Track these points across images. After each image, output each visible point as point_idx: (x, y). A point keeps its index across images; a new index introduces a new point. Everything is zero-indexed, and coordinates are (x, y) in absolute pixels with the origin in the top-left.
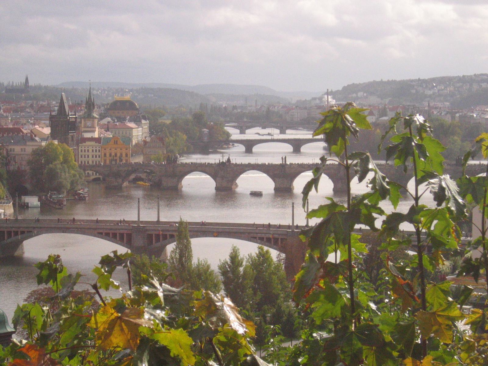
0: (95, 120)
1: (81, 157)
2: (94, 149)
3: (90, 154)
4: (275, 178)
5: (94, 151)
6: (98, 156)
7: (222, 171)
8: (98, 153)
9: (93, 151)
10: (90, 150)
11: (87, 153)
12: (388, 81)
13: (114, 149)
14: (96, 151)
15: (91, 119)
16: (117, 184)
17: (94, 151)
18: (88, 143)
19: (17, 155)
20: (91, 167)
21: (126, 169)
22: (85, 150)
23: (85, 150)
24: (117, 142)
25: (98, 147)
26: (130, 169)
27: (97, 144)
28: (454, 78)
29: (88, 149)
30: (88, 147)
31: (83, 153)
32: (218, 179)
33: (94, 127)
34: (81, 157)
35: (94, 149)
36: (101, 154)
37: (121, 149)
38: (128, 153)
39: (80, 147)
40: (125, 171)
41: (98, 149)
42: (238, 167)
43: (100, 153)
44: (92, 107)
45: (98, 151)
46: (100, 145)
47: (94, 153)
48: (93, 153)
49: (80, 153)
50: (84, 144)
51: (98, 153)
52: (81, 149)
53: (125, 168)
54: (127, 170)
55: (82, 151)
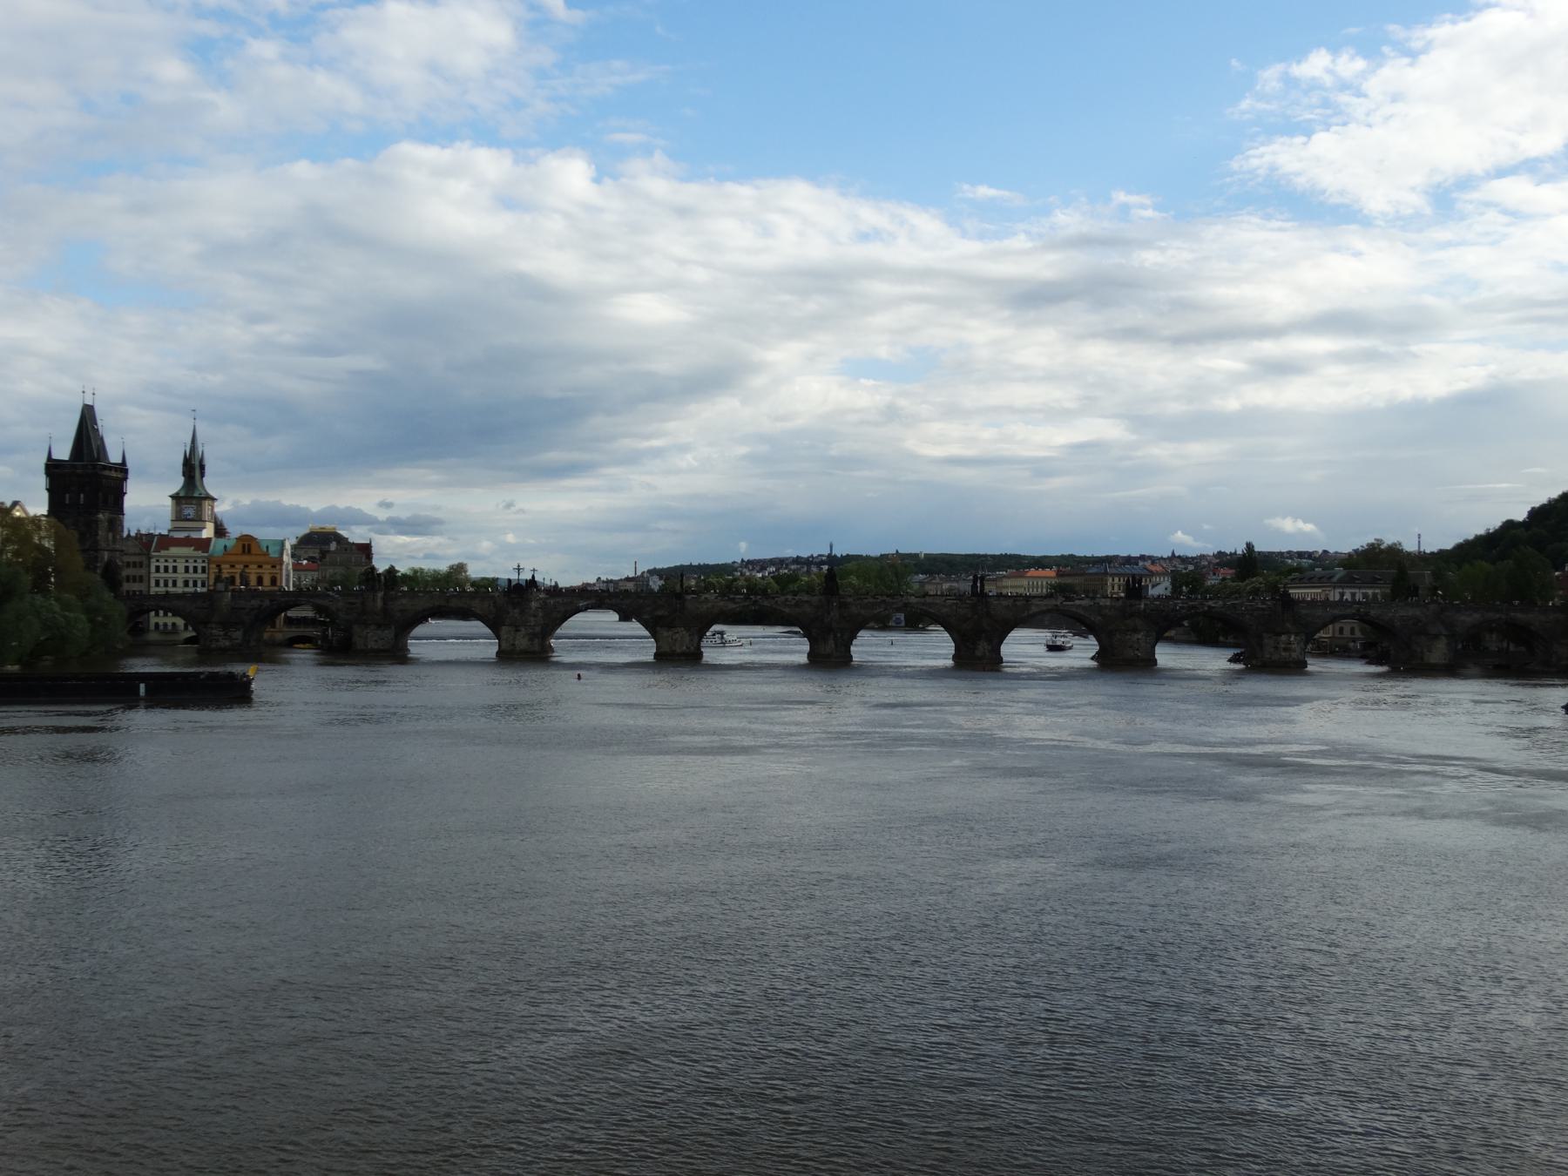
0: (203, 502)
1: (157, 584)
2: (191, 565)
3: (181, 576)
4: (658, 629)
5: (191, 570)
6: (199, 584)
7: (515, 608)
8: (200, 576)
9: (187, 569)
10: (181, 568)
11: (170, 575)
12: (699, 564)
14: (195, 568)
15: (194, 502)
16: (227, 643)
17: (191, 570)
18: (174, 551)
20: (167, 603)
21: (256, 603)
22: (166, 569)
23: (166, 569)
24: (249, 545)
25: (199, 561)
26: (267, 603)
27: (200, 553)
28: (787, 559)
29: (175, 564)
31: (162, 575)
32: (504, 629)
34: (157, 584)
35: (191, 565)
36: (208, 578)
38: (278, 576)
39: (153, 560)
41: (200, 565)
42: (560, 600)
43: (205, 576)
45: (200, 570)
46: (206, 554)
47: (191, 575)
49: (154, 575)
50: (163, 553)
51: (200, 576)
52: (158, 564)
53: (253, 602)
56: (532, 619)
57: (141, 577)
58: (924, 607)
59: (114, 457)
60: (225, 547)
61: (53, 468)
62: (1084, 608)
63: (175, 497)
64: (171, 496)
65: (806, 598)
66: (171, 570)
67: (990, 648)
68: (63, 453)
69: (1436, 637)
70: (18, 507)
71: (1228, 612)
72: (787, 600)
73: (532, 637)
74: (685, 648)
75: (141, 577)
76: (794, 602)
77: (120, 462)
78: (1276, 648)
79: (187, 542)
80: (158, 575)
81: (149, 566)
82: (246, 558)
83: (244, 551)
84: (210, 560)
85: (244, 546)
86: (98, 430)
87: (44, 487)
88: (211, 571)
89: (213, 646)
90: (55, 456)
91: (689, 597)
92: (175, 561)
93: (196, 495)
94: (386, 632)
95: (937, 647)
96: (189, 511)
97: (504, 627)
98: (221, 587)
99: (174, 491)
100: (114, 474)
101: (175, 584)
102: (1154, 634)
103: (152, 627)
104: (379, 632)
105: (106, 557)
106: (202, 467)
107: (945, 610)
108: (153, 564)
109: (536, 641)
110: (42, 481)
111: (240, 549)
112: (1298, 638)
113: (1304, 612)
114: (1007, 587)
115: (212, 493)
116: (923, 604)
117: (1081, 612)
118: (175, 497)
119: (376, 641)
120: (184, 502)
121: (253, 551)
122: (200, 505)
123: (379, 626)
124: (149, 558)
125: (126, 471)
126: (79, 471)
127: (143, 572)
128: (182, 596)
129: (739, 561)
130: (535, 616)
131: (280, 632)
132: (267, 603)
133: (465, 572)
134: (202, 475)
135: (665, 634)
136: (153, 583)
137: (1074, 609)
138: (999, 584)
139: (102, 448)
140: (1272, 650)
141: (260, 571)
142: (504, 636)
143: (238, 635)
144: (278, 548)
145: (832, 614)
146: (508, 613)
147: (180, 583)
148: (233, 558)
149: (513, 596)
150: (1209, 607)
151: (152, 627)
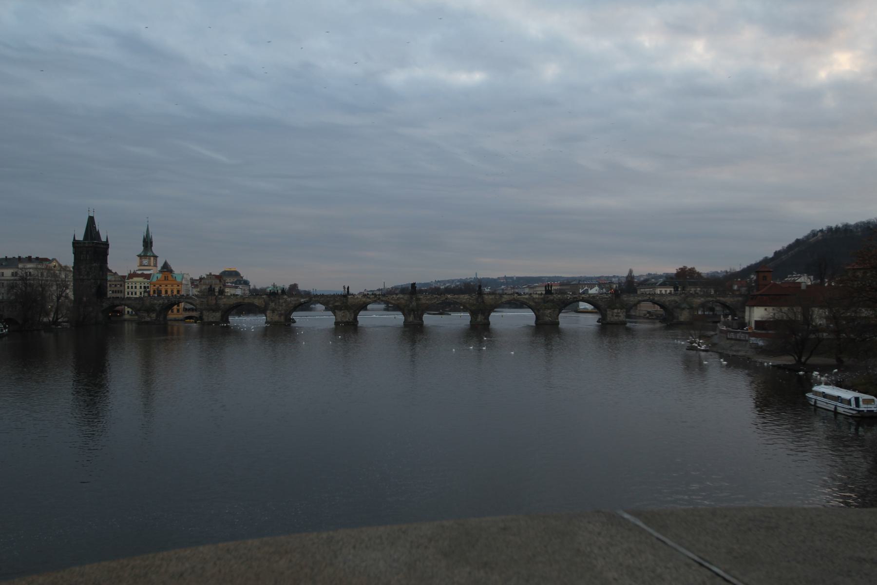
1: (128, 294)
4: (336, 311)
7: (272, 302)
9: (141, 287)
10: (138, 287)
11: (134, 290)
13: (164, 286)
15: (148, 258)
16: (148, 319)
18: (135, 279)
19: (7, 280)
21: (161, 301)
22: (132, 287)
23: (132, 287)
24: (168, 277)
25: (146, 283)
26: (166, 301)
27: (146, 280)
28: (455, 280)
30: (136, 284)
31: (130, 290)
33: (150, 266)
34: (128, 294)
37: (172, 286)
39: (126, 283)
40: (160, 304)
44: (149, 245)
46: (149, 281)
48: (141, 290)
49: (127, 290)
50: (131, 280)
53: (160, 301)
54: (161, 303)
55: (128, 287)
56: (280, 307)
57: (121, 291)
58: (455, 300)
59: (104, 239)
60: (157, 277)
61: (76, 243)
62: (526, 299)
63: (139, 256)
64: (138, 256)
65: (401, 296)
66: (134, 287)
67: (484, 317)
68: (80, 237)
69: (683, 309)
70: (54, 261)
71: (591, 300)
72: (393, 297)
73: (280, 315)
74: (347, 319)
75: (121, 291)
76: (396, 298)
77: (105, 240)
78: (612, 315)
79: (142, 275)
80: (128, 290)
81: (125, 286)
82: (166, 282)
83: (165, 279)
84: (151, 283)
85: (165, 277)
86: (95, 227)
87: (72, 252)
88: (151, 288)
89: (143, 320)
90: (77, 239)
91: (350, 297)
92: (136, 284)
93: (148, 255)
94: (217, 314)
95: (461, 319)
96: (145, 262)
97: (268, 311)
98: (146, 294)
99: (139, 253)
100: (102, 246)
101: (136, 294)
102: (558, 310)
103: (126, 312)
104: (214, 314)
105: (99, 283)
106: (151, 243)
107: (464, 301)
108: (126, 286)
109: (282, 317)
110: (70, 249)
111: (164, 279)
112: (622, 311)
113: (625, 299)
114: (538, 291)
115: (156, 254)
116: (455, 298)
117: (525, 301)
118: (139, 256)
119: (212, 318)
120: (143, 258)
121: (169, 279)
122: (150, 259)
123: (214, 311)
124: (125, 283)
125: (108, 245)
126: (87, 245)
127: (122, 288)
128: (129, 298)
129: (434, 281)
130: (282, 306)
131: (181, 314)
132: (166, 301)
133: (297, 287)
134: (151, 246)
135: (339, 313)
136: (126, 293)
137: (522, 300)
138: (535, 289)
139: (98, 233)
140: (611, 316)
141: (172, 288)
142: (268, 315)
143: (154, 316)
144: (181, 277)
145: (413, 303)
146: (270, 304)
147: (138, 294)
148: (161, 282)
149: (271, 297)
150: (583, 297)
151: (126, 312)
